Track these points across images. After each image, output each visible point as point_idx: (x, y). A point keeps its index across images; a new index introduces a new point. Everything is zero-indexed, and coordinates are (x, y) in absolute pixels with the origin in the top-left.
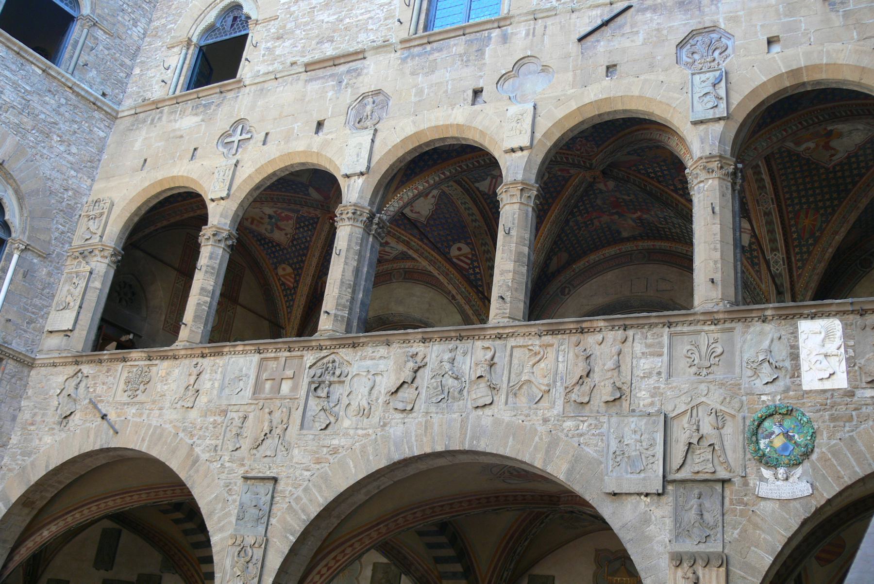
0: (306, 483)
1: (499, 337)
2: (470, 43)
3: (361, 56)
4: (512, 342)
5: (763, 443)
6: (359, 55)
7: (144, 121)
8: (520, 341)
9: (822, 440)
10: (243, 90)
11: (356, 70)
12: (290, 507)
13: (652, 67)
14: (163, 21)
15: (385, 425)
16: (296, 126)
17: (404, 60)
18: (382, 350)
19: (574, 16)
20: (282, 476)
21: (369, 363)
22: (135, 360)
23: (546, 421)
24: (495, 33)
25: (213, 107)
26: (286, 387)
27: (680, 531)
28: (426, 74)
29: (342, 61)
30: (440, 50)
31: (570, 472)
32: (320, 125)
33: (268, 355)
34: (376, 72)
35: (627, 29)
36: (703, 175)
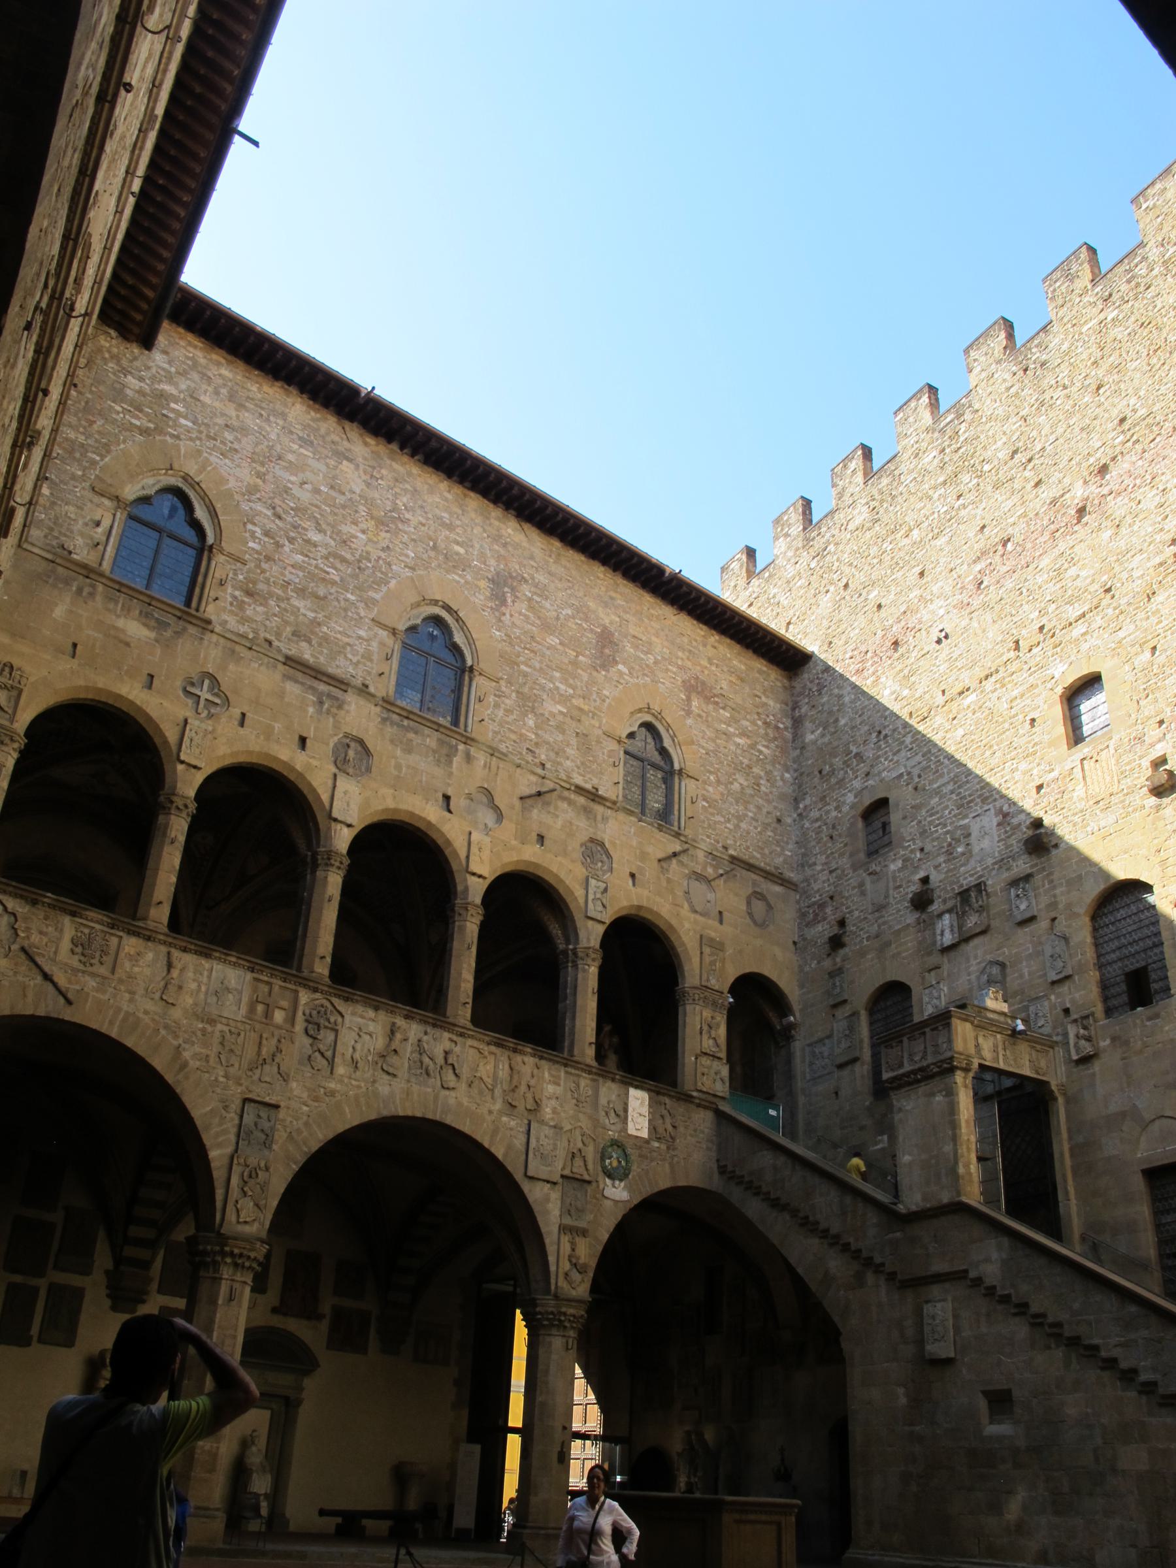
0: (305, 1118)
1: (462, 1035)
2: (441, 742)
3: (343, 687)
4: (470, 1042)
5: (608, 1161)
6: (342, 684)
7: (67, 582)
8: (475, 1043)
9: (634, 1167)
10: (208, 636)
11: (337, 699)
12: (290, 1137)
13: (565, 853)
14: (81, 439)
15: (374, 1082)
16: (276, 725)
17: (384, 720)
18: (371, 1013)
19: (518, 770)
20: (282, 1104)
21: (360, 1020)
22: (92, 921)
24: (461, 747)
25: (168, 634)
26: (279, 1016)
27: (567, 1211)
28: (404, 750)
30: (416, 733)
31: (505, 1155)
32: (303, 741)
33: (261, 977)
34: (359, 716)
35: (552, 809)
36: (589, 962)
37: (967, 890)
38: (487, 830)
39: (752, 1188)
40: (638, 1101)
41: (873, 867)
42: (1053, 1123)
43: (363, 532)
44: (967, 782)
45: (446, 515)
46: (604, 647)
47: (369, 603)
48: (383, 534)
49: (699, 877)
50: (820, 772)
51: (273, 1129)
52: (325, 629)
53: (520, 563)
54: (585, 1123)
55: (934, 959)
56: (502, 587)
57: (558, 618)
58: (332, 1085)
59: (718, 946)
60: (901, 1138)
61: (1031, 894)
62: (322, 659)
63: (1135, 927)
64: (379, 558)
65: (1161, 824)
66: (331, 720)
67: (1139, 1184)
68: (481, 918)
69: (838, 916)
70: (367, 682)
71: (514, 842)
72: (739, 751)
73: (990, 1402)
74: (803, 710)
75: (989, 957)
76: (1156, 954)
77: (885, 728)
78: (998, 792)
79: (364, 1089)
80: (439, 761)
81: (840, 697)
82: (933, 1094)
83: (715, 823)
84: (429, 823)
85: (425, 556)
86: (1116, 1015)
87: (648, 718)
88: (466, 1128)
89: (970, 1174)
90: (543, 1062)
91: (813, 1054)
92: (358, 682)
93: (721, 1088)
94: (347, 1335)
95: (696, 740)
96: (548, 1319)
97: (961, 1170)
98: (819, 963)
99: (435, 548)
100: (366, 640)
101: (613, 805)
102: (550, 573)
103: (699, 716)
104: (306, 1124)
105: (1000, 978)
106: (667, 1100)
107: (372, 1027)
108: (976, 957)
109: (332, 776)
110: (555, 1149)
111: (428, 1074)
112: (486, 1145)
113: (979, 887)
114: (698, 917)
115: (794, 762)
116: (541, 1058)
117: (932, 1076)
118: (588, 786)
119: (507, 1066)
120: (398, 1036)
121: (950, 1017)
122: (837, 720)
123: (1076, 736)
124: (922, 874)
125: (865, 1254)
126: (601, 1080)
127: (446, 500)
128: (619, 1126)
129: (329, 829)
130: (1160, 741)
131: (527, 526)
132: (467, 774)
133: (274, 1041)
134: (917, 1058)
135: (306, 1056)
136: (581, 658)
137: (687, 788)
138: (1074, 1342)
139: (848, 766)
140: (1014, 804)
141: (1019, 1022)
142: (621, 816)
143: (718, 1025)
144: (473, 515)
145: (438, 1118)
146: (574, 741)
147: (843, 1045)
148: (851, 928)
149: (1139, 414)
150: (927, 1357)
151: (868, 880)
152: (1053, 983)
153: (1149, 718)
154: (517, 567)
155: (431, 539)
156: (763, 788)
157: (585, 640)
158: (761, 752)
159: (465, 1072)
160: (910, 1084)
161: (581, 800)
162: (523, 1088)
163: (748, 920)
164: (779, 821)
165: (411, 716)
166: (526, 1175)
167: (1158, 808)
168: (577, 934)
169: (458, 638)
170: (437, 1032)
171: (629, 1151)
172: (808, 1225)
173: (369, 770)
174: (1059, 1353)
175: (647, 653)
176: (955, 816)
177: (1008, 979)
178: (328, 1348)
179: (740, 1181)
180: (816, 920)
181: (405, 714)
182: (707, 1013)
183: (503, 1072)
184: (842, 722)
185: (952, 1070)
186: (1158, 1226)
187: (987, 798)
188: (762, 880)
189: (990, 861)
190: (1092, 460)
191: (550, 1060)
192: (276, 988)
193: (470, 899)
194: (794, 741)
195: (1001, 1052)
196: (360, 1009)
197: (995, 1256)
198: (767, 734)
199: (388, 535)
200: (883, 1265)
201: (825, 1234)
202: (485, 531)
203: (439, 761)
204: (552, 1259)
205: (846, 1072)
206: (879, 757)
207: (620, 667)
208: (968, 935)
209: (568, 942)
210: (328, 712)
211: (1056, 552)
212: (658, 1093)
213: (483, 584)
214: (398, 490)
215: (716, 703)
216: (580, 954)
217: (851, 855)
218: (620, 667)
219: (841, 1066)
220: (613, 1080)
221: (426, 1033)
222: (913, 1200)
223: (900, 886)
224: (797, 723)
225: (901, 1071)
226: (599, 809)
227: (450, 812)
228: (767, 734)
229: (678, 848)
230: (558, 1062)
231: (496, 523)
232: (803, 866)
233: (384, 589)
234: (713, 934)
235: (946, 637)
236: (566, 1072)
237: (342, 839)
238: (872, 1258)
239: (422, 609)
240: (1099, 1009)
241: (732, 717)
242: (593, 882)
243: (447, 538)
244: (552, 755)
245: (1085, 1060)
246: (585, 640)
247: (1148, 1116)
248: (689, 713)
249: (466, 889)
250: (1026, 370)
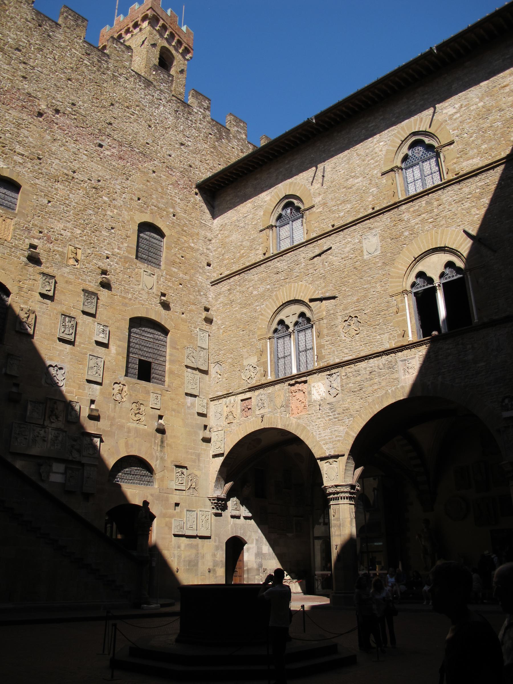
65: (25, 271)
130: (37, 239)
149: (81, 111)
153: (36, 226)
167: (26, 265)
190: (54, 101)
211: (20, 115)
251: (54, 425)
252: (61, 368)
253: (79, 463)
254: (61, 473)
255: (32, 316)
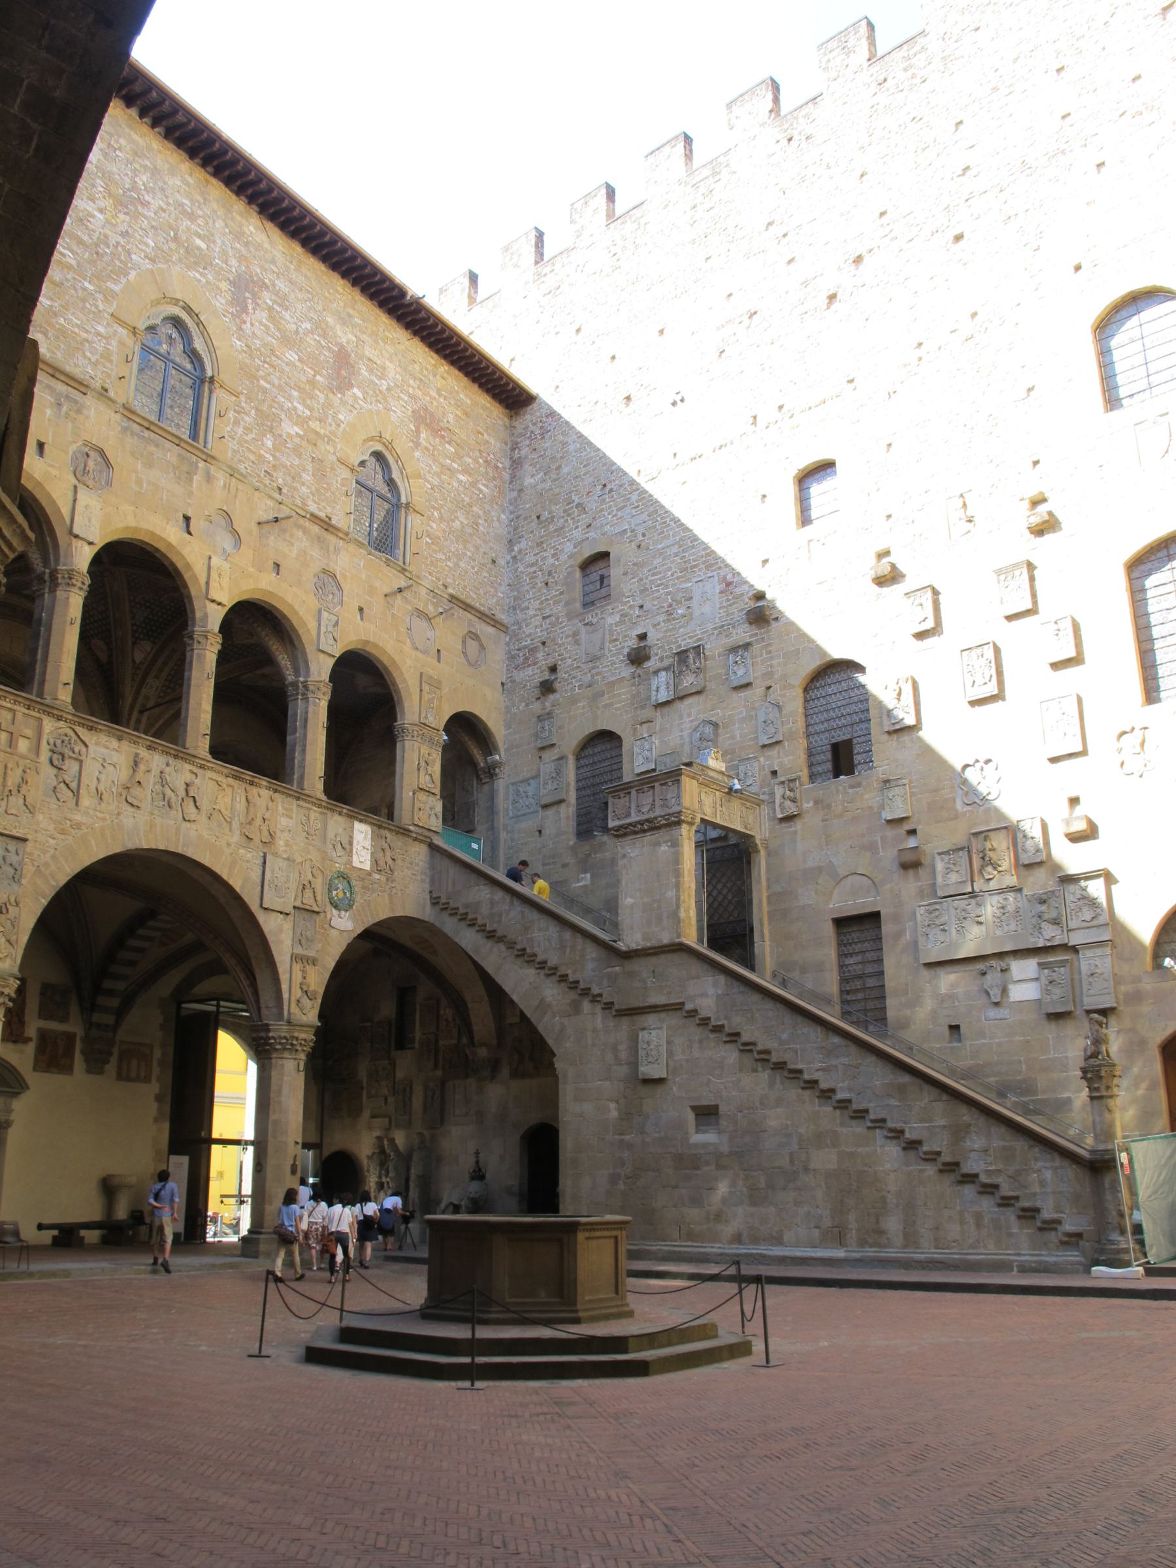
0: (52, 851)
1: (202, 767)
3: (82, 389)
4: (209, 774)
8: (214, 776)
11: (76, 402)
15: (119, 814)
17: (125, 430)
18: (115, 743)
19: (256, 493)
21: (103, 750)
23: (229, 845)
24: (201, 464)
26: (23, 746)
29: (62, 378)
30: (157, 446)
31: (243, 887)
37: (685, 651)
38: (227, 556)
39: (467, 919)
40: (362, 833)
41: (589, 618)
42: (754, 874)
43: (101, 211)
44: (693, 547)
45: (186, 202)
46: (340, 368)
47: (109, 296)
48: (122, 216)
49: (421, 614)
50: (538, 517)
51: (21, 863)
52: (62, 320)
53: (262, 268)
54: (315, 856)
55: (648, 713)
56: (244, 290)
57: (297, 332)
58: (78, 817)
59: (436, 685)
60: (624, 882)
61: (749, 662)
62: (59, 355)
63: (844, 702)
64: (118, 243)
66: (70, 425)
67: (829, 930)
68: (219, 647)
69: (550, 661)
70: (106, 386)
71: (251, 569)
72: (461, 489)
73: (697, 1115)
74: (523, 453)
75: (702, 717)
76: (861, 730)
77: (611, 482)
78: (723, 561)
79: (109, 822)
80: (179, 478)
81: (565, 444)
82: (658, 844)
83: (437, 560)
84: (170, 545)
85: (165, 248)
86: (819, 780)
87: (379, 447)
88: (206, 861)
89: (689, 917)
90: (277, 795)
91: (518, 793)
92: (97, 384)
93: (436, 823)
94: (53, 1055)
95: (425, 474)
96: (280, 1043)
97: (682, 915)
98: (527, 705)
99: (176, 239)
100: (105, 338)
101: (345, 536)
102: (291, 282)
103: (427, 449)
104: (53, 857)
105: (712, 736)
106: (388, 835)
107: (115, 757)
108: (689, 715)
109: (72, 488)
110: (288, 881)
111: (170, 806)
112: (225, 877)
113: (698, 650)
114: (419, 654)
115: (511, 504)
116: (276, 791)
117: (658, 828)
118: (322, 515)
119: (244, 799)
120: (142, 767)
121: (680, 775)
122: (559, 467)
123: (805, 519)
124: (640, 631)
125: (582, 985)
126: (329, 812)
127: (188, 184)
128: (345, 859)
129: (70, 545)
131: (269, 225)
132: (208, 494)
133: (19, 772)
134: (645, 810)
135: (51, 787)
136: (318, 377)
137: (413, 523)
138: (780, 1066)
139: (569, 515)
140: (739, 574)
141: (736, 781)
142: (352, 548)
143: (434, 761)
144: (215, 206)
145: (180, 851)
146: (309, 467)
147: (549, 787)
148: (561, 674)
150: (640, 1077)
151: (583, 630)
152: (764, 746)
154: (258, 271)
155: (171, 228)
156: (481, 528)
157: (322, 358)
158: (481, 491)
159: (204, 803)
160: (635, 833)
161: (315, 529)
162: (259, 821)
163: (463, 660)
164: (494, 562)
165: (152, 428)
166: (261, 906)
168: (307, 667)
169: (198, 344)
170: (179, 764)
171: (353, 883)
172: (525, 956)
173: (109, 483)
174: (765, 1075)
175: (381, 378)
176: (678, 578)
177: (720, 739)
178: (34, 1070)
179: (454, 912)
180: (526, 663)
181: (147, 425)
182: (425, 750)
183: (241, 805)
184: (565, 470)
185: (679, 823)
186: (841, 966)
187: (711, 565)
188: (476, 620)
189: (710, 626)
191: (284, 793)
192: (19, 716)
193: (209, 628)
194: (511, 482)
195: (719, 808)
196: (103, 738)
197: (711, 991)
198: (487, 473)
199: (127, 218)
200: (600, 995)
201: (542, 965)
202: (226, 225)
203: (179, 478)
204: (285, 987)
205: (550, 812)
206: (602, 510)
207: (355, 390)
208: (682, 694)
209: (297, 672)
210: (67, 416)
212: (380, 827)
213: (224, 286)
214: (137, 166)
215: (443, 437)
216: (311, 688)
217: (567, 604)
218: (355, 390)
219: (545, 807)
220: (340, 814)
221: (168, 765)
222: (632, 940)
223: (616, 640)
224: (516, 464)
225: (628, 821)
226: (331, 539)
227: (190, 533)
228: (487, 473)
229: (403, 584)
230: (290, 795)
231: (239, 218)
232: (515, 609)
233: (124, 281)
234: (431, 672)
235: (682, 400)
236: (298, 806)
237: (82, 557)
238: (589, 989)
239: (161, 308)
240: (804, 774)
241: (456, 452)
242: (325, 615)
243: (188, 229)
244: (288, 479)
245: (789, 819)
246: (322, 358)
247: (842, 872)
248: (417, 445)
249: (206, 616)
250: (790, 140)
251: (993, 885)
252: (988, 761)
253: (1064, 947)
254: (1032, 980)
255: (908, 690)
